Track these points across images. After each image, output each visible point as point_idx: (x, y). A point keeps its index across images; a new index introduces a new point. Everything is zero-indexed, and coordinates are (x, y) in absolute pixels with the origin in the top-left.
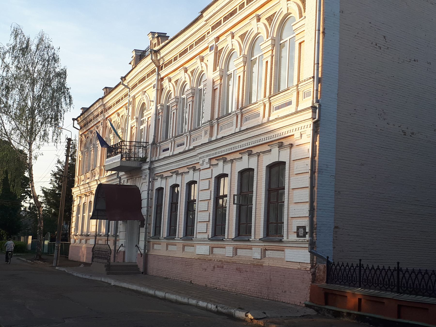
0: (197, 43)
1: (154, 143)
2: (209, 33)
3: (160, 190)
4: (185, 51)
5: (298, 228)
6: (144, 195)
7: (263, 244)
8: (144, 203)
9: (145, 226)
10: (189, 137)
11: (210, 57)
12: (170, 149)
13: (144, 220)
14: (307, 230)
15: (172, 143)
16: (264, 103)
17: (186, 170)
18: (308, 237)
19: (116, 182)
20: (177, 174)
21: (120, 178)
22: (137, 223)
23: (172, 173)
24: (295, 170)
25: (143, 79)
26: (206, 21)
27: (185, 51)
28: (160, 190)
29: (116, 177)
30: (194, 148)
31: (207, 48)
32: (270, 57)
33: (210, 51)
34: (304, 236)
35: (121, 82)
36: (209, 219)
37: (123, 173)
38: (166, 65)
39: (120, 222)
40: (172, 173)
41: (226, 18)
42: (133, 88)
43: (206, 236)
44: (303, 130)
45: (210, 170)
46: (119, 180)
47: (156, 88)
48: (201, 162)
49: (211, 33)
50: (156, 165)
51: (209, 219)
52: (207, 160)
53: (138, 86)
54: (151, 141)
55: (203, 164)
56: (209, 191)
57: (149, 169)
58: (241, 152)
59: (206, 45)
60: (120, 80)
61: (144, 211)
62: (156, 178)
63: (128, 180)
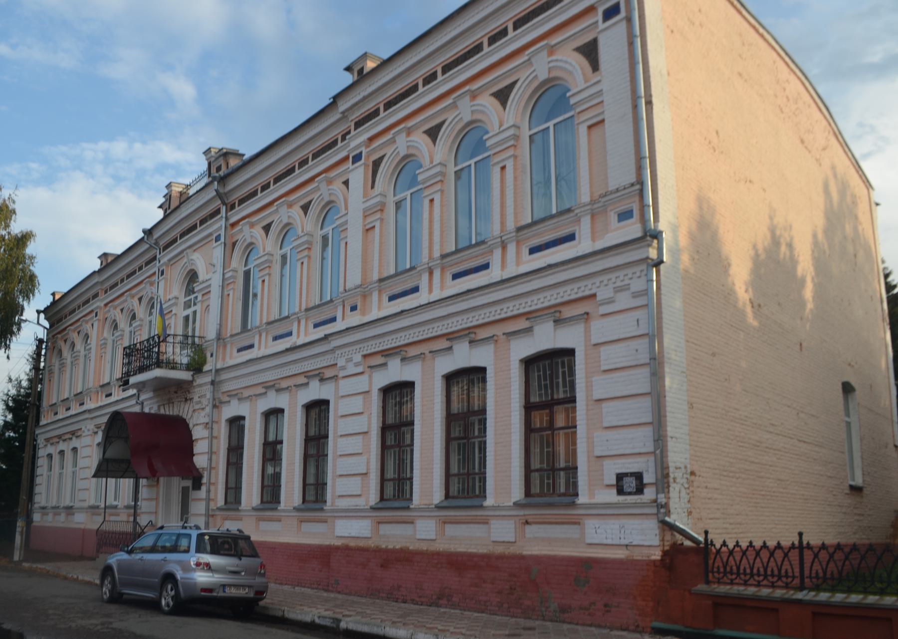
0: (316, 155)
1: (219, 337)
2: (349, 132)
3: (237, 423)
4: (291, 171)
5: (620, 477)
6: (198, 433)
7: (522, 513)
8: (200, 447)
9: (204, 488)
11: (358, 175)
12: (256, 346)
13: (200, 477)
14: (648, 478)
16: (503, 242)
17: (302, 380)
18: (649, 494)
19: (137, 409)
20: (279, 390)
22: (177, 483)
23: (267, 388)
24: (602, 363)
26: (343, 113)
27: (291, 171)
29: (134, 402)
30: (326, 337)
31: (346, 158)
33: (353, 163)
34: (640, 490)
35: (143, 238)
36: (368, 469)
38: (242, 201)
39: (143, 482)
40: (267, 388)
41: (389, 105)
42: (166, 247)
43: (361, 502)
44: (619, 284)
45: (365, 377)
47: (222, 239)
48: (341, 362)
49: (353, 133)
50: (224, 376)
51: (368, 469)
52: (358, 358)
53: (179, 242)
54: (211, 334)
57: (213, 383)
58: (451, 337)
59: (343, 154)
60: (142, 235)
61: (200, 461)
62: (227, 399)
63: (159, 407)
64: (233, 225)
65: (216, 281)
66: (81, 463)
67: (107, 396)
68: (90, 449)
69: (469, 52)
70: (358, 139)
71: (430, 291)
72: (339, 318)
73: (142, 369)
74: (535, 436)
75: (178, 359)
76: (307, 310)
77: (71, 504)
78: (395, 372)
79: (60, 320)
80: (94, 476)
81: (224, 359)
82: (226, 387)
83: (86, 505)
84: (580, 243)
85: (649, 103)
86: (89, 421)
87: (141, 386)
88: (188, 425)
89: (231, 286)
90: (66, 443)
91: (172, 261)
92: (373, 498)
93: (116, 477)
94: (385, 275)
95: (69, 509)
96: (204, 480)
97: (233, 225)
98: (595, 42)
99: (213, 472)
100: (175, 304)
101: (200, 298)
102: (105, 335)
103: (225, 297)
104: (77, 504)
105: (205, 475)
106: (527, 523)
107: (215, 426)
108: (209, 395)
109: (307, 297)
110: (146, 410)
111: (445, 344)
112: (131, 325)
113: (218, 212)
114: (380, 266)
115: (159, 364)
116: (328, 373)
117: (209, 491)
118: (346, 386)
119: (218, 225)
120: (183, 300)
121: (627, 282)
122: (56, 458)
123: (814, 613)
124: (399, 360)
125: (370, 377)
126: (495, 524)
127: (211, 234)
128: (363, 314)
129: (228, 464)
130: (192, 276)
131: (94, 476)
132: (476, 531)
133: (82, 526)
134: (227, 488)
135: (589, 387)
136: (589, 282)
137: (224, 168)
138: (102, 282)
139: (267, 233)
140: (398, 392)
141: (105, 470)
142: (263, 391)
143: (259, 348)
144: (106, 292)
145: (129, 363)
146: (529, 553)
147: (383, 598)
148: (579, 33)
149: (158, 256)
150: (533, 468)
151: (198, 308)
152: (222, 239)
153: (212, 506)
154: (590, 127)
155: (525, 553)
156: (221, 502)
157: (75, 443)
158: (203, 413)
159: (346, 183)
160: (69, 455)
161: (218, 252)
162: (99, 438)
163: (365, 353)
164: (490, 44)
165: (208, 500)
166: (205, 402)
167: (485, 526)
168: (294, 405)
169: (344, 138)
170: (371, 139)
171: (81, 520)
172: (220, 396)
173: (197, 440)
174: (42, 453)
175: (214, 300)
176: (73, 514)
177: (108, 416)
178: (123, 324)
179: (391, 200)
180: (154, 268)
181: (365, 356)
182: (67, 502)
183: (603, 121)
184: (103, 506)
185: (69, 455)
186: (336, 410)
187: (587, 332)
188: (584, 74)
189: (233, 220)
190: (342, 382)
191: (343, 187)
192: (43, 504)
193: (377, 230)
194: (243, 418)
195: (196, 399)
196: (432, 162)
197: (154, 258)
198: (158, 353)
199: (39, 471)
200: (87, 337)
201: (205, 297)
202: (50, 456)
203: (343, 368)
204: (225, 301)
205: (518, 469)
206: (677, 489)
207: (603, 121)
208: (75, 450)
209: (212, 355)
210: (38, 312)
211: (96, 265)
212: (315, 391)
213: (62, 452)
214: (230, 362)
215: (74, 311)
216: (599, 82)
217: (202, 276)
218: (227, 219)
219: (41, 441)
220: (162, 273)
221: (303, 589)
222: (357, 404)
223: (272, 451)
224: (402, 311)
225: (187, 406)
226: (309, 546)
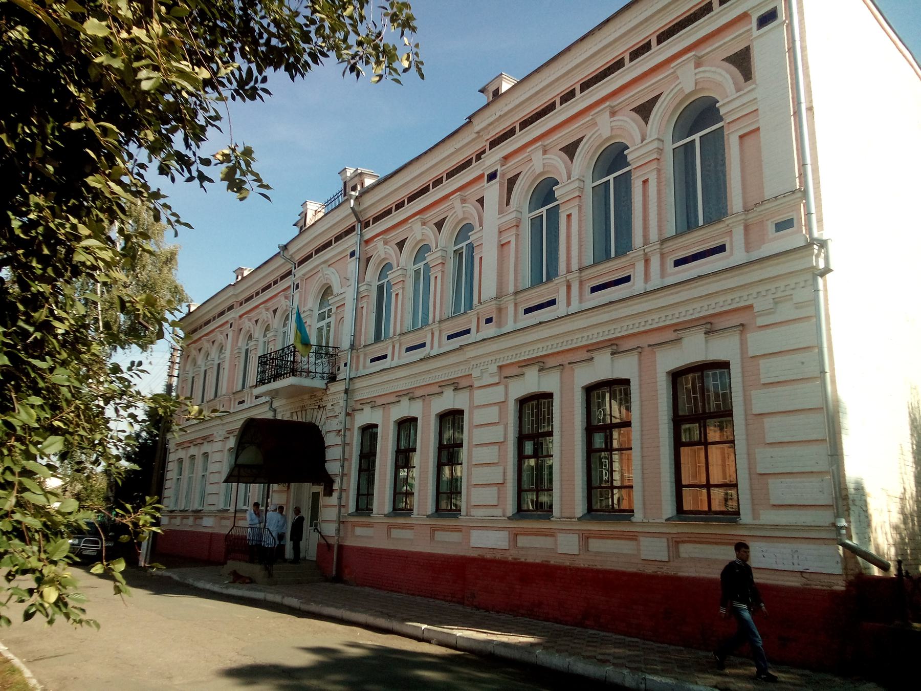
1: (352, 347)
2: (484, 152)
3: (369, 431)
6: (330, 439)
8: (333, 454)
9: (335, 495)
10: (437, 334)
11: (493, 192)
12: (389, 356)
15: (394, 347)
16: (645, 254)
17: (436, 389)
19: (269, 416)
21: (275, 411)
24: (761, 376)
25: (329, 244)
26: (478, 133)
28: (369, 431)
31: (482, 176)
32: (655, 172)
36: (504, 479)
37: (284, 402)
38: (376, 219)
41: (525, 124)
42: (300, 263)
45: (501, 388)
48: (476, 373)
50: (358, 384)
51: (504, 479)
52: (493, 368)
54: (345, 344)
55: (482, 376)
56: (500, 428)
57: (346, 391)
61: (333, 468)
62: (360, 407)
64: (367, 242)
65: (350, 294)
66: (213, 468)
67: (240, 403)
68: (221, 454)
69: (609, 68)
70: (492, 160)
71: (569, 304)
72: (473, 331)
73: (277, 377)
74: (684, 451)
75: (312, 369)
77: (200, 508)
78: (532, 383)
79: (195, 331)
80: (225, 481)
81: (357, 369)
82: (358, 396)
83: (213, 508)
84: (732, 254)
85: (810, 109)
86: (221, 427)
87: (274, 394)
88: (320, 432)
89: (365, 300)
90: (197, 448)
91: (307, 278)
92: (510, 508)
93: (246, 483)
94: (520, 288)
95: (198, 514)
96: (336, 486)
97: (367, 242)
98: (747, 50)
99: (345, 478)
100: (310, 316)
101: (334, 310)
102: (239, 344)
103: (359, 310)
104: (206, 508)
105: (337, 481)
107: (348, 433)
108: (342, 403)
109: (441, 310)
110: (279, 417)
111: (586, 355)
112: (265, 336)
114: (516, 280)
115: (294, 372)
116: (463, 383)
117: (340, 498)
118: (480, 396)
119: (352, 241)
120: (316, 312)
121: (787, 293)
122: (186, 464)
124: (536, 372)
125: (506, 387)
126: (645, 542)
127: (345, 250)
128: (499, 325)
129: (361, 470)
130: (327, 291)
131: (225, 481)
132: (624, 547)
133: (210, 531)
134: (358, 495)
135: (747, 401)
136: (744, 293)
137: (359, 188)
138: (236, 295)
139: (401, 249)
140: (535, 402)
141: (237, 474)
142: (397, 399)
143: (393, 359)
144: (241, 304)
145: (263, 372)
146: (686, 574)
147: (523, 615)
148: (731, 44)
149: (293, 271)
150: (684, 483)
151: (332, 319)
152: (357, 255)
153: (343, 510)
154: (741, 137)
155: (680, 574)
156: (352, 508)
157: (206, 448)
158: (335, 421)
159: (481, 201)
160: (199, 461)
161: (352, 266)
162: (232, 443)
163: (501, 364)
164: (631, 60)
165: (340, 506)
166: (338, 410)
167: (634, 543)
168: (427, 415)
169: (478, 157)
170: (506, 158)
171: (208, 524)
172: (353, 404)
173: (329, 447)
174: (172, 457)
175: (349, 314)
176: (201, 518)
177: (241, 422)
178: (257, 333)
179: (527, 217)
180: (287, 282)
181: (500, 367)
182: (196, 506)
183: (758, 129)
185: (199, 461)
186: (470, 419)
187: (743, 344)
188: (735, 83)
189: (367, 237)
190: (477, 393)
191: (479, 205)
192: (172, 508)
193: (513, 245)
194: (376, 426)
195: (329, 406)
196: (569, 178)
197: (289, 273)
198: (293, 362)
199: (169, 475)
200: (221, 348)
201: (340, 310)
202: (180, 461)
203: (479, 378)
204: (359, 314)
205: (668, 484)
206: (857, 512)
207: (758, 129)
208: (206, 455)
209: (345, 365)
212: (448, 401)
213: (193, 457)
214: (362, 372)
216: (753, 89)
217: (336, 289)
218: (361, 235)
219: (171, 446)
220: (297, 287)
221: (438, 602)
222: (492, 414)
223: (403, 457)
224: (540, 323)
225: (320, 413)
226: (443, 556)
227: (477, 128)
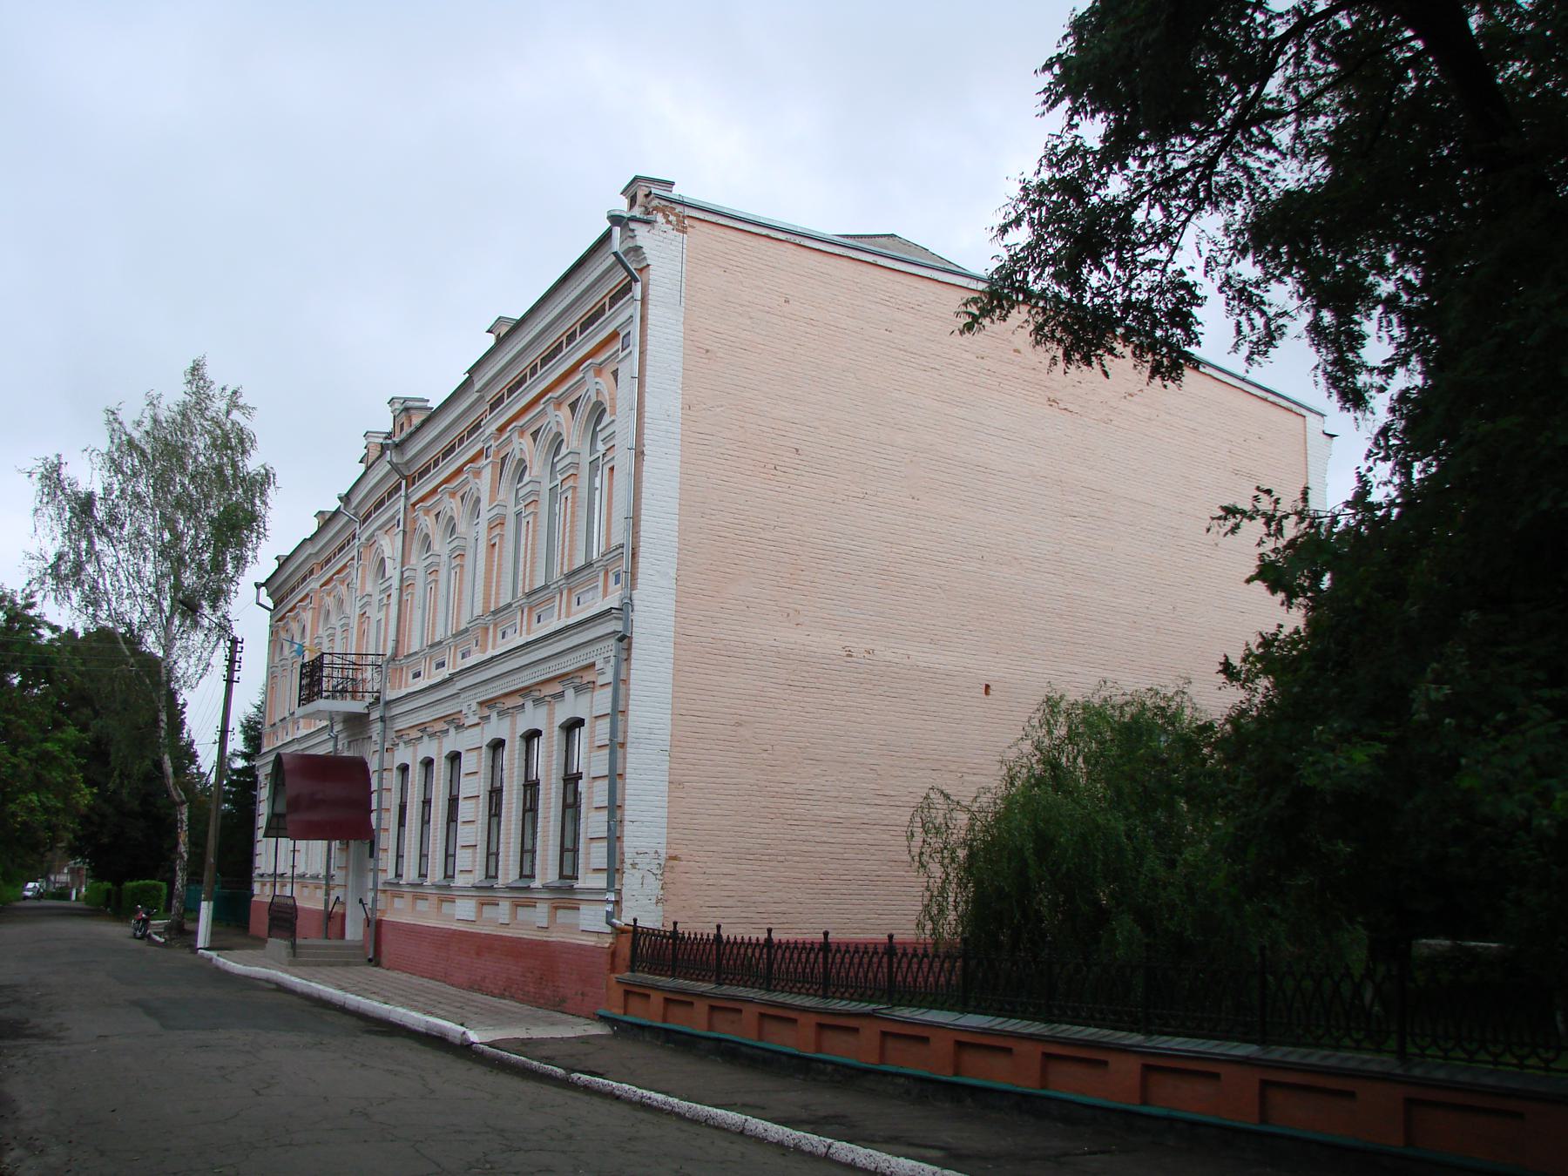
1: (394, 658)
11: (487, 469)
20: (431, 736)
25: (381, 503)
38: (421, 475)
39: (336, 844)
46: (331, 743)
50: (396, 711)
52: (474, 706)
57: (382, 719)
64: (414, 505)
76: (454, 636)
82: (401, 724)
85: (639, 454)
106: (556, 908)
113: (398, 488)
123: (666, 1000)
170: (501, 430)
181: (481, 704)
184: (289, 873)
189: (414, 499)
210: (258, 586)
211: (312, 526)
215: (293, 590)
218: (407, 497)
227: (477, 386)
